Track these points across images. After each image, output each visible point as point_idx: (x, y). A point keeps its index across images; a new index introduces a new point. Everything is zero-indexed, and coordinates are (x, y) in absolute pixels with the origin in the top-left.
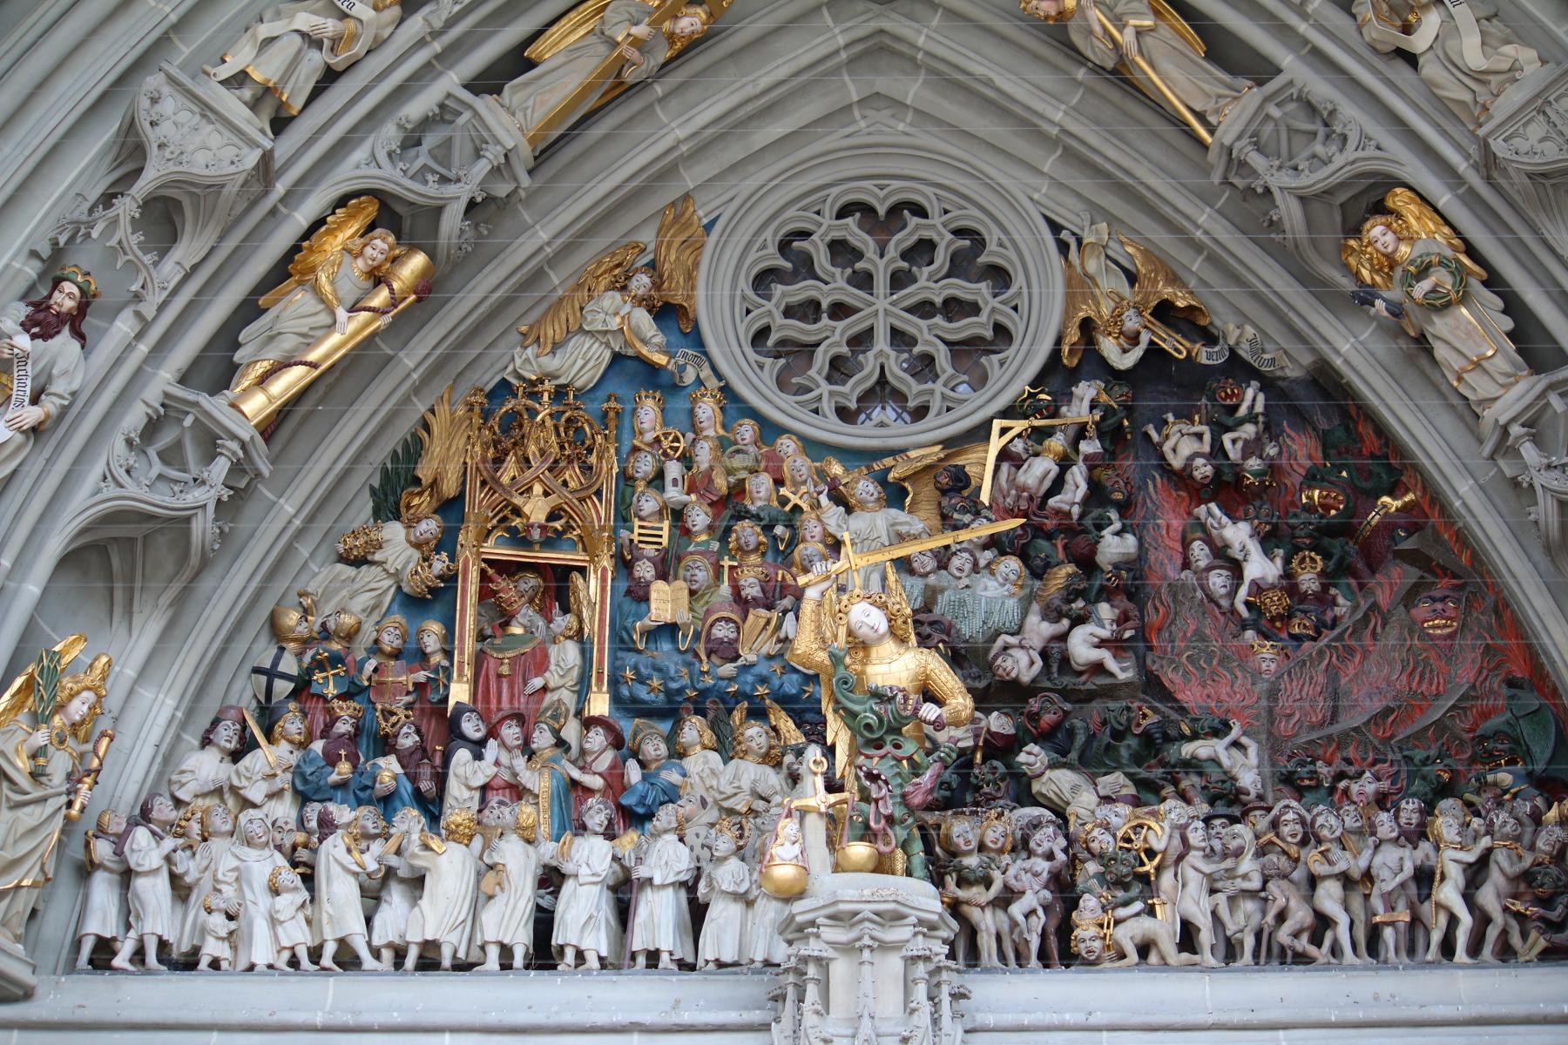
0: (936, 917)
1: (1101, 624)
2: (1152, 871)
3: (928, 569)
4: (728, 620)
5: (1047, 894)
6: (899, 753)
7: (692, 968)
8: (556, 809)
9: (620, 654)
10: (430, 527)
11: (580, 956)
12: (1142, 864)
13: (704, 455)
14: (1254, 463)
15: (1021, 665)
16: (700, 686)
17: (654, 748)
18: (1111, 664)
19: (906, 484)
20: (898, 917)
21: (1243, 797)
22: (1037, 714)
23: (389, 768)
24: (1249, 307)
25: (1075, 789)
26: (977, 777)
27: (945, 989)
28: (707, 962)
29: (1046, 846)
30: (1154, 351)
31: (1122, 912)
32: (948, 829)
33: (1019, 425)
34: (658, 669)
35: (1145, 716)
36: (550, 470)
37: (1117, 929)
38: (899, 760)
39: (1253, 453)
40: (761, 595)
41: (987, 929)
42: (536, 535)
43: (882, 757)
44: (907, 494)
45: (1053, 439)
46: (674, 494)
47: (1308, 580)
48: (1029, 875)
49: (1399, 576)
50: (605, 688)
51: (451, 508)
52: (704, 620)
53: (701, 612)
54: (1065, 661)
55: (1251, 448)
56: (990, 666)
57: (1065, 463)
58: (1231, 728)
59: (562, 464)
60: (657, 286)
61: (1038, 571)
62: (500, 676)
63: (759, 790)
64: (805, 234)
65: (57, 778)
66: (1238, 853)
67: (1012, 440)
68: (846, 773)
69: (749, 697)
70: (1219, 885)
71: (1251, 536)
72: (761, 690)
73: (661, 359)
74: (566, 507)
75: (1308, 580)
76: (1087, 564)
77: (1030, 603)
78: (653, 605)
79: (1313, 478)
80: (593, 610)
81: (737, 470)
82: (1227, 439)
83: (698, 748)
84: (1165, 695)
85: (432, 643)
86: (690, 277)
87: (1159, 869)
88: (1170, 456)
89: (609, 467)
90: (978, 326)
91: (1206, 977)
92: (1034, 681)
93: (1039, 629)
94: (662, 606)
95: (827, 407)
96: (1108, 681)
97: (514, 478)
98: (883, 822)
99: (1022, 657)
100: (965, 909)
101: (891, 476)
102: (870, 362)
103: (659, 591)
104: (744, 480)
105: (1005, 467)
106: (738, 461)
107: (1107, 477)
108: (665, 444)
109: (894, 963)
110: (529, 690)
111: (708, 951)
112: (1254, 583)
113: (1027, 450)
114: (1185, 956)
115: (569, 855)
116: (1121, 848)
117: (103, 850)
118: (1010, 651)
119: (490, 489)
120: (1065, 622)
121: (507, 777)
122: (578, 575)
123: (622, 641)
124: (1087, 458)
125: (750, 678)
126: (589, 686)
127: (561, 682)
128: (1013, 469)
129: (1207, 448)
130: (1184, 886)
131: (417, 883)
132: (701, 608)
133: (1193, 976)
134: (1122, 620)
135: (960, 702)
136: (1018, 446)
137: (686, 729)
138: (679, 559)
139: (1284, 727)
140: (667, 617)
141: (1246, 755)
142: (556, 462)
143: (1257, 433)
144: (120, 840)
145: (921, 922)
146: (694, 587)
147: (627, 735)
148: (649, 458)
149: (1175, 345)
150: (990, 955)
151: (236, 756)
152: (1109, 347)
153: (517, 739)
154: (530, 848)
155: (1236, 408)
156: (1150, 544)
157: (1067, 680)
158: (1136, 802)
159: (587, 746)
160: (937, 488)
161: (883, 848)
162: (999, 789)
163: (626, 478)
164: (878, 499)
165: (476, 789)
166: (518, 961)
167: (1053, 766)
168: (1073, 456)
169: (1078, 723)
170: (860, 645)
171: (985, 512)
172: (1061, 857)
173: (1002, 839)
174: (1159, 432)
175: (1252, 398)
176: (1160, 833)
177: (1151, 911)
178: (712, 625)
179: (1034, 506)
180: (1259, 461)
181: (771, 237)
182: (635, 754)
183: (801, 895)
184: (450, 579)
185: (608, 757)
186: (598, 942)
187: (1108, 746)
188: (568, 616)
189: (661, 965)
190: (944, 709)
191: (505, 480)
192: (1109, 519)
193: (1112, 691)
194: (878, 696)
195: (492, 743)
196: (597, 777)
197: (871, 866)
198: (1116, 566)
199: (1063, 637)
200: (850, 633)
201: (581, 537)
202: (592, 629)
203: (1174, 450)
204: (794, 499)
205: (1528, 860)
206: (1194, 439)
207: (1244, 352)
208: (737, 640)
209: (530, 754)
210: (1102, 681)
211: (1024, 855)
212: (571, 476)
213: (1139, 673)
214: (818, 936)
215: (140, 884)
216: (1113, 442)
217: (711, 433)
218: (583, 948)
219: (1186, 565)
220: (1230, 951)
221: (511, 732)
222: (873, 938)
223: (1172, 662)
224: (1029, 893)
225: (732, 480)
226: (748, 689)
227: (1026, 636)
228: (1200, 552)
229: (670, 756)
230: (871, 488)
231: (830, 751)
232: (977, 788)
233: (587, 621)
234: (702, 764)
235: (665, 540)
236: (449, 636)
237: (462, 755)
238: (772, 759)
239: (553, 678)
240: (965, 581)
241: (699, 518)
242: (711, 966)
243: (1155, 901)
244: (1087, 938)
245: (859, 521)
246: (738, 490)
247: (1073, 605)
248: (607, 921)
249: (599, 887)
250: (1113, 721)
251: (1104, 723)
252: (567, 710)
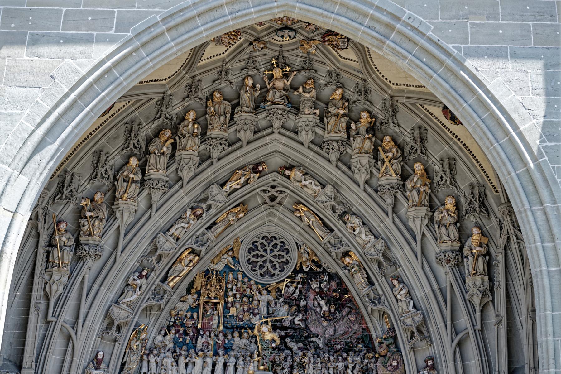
10: (196, 296)
13: (239, 285)
14: (325, 289)
15: (287, 324)
17: (229, 337)
18: (301, 324)
23: (188, 338)
24: (326, 261)
25: (294, 346)
30: (311, 269)
33: (289, 280)
46: (234, 292)
47: (332, 310)
49: (346, 310)
51: (199, 293)
54: (294, 322)
60: (233, 254)
61: (290, 306)
64: (257, 242)
65: (140, 348)
73: (233, 267)
75: (332, 310)
76: (298, 306)
79: (335, 291)
84: (309, 329)
85: (195, 316)
86: (238, 252)
89: (224, 285)
90: (284, 260)
93: (290, 318)
95: (259, 274)
102: (266, 266)
103: (232, 309)
106: (245, 286)
117: (145, 357)
131: (194, 363)
132: (238, 311)
134: (303, 316)
136: (289, 284)
139: (327, 335)
144: (148, 355)
149: (314, 268)
151: (164, 336)
152: (304, 267)
155: (322, 280)
172: (291, 363)
175: (326, 277)
177: (304, 371)
181: (251, 242)
184: (198, 305)
193: (300, 329)
198: (303, 307)
199: (294, 319)
205: (362, 366)
207: (325, 268)
210: (299, 327)
215: (151, 364)
219: (314, 305)
228: (316, 303)
234: (237, 339)
236: (198, 315)
237: (200, 337)
239: (214, 322)
241: (238, 296)
245: (263, 297)
246: (244, 291)
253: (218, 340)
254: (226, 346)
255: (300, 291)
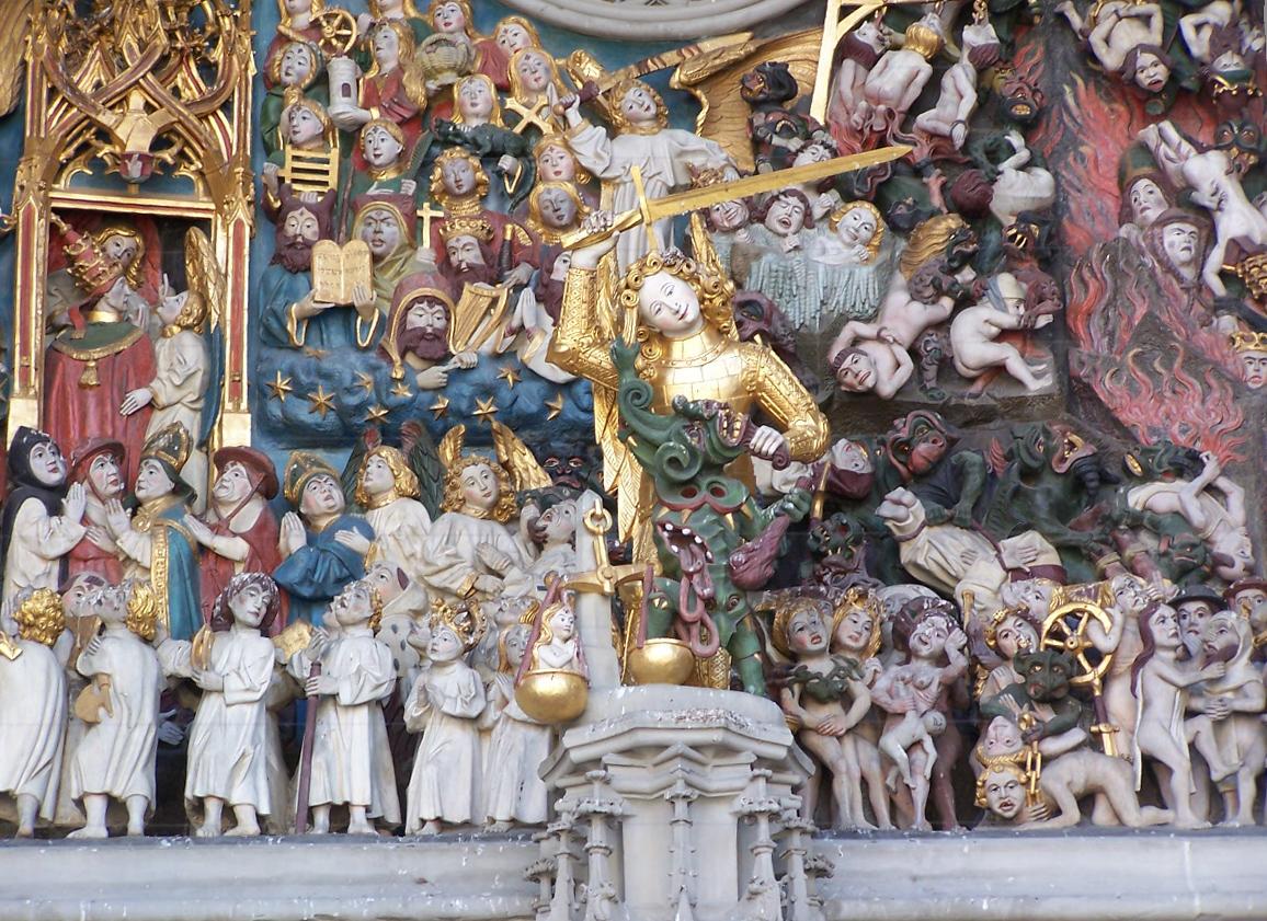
0: (782, 753)
1: (1000, 304)
2: (1097, 682)
3: (736, 222)
4: (432, 301)
5: (937, 719)
6: (721, 502)
7: (399, 831)
8: (176, 590)
9: (266, 353)
11: (228, 812)
12: (1083, 672)
13: (389, 49)
14: (1229, 62)
16: (392, 401)
17: (323, 497)
18: (1016, 366)
19: (698, 92)
20: (725, 750)
21: (1224, 570)
22: (907, 443)
25: (968, 557)
26: (817, 539)
27: (797, 866)
28: (423, 822)
29: (936, 644)
31: (1052, 745)
32: (787, 617)
34: (327, 376)
35: (1072, 445)
36: (154, 70)
37: (1048, 771)
38: (723, 513)
39: (1226, 47)
40: (481, 262)
41: (848, 771)
42: (135, 170)
43: (695, 509)
44: (700, 107)
45: (923, 22)
46: (344, 107)
48: (911, 688)
50: (244, 405)
52: (395, 301)
53: (390, 288)
54: (946, 364)
55: (1226, 38)
56: (833, 371)
57: (940, 61)
58: (1203, 465)
59: (173, 61)
61: (900, 225)
62: (83, 387)
63: (487, 560)
66: (1228, 654)
67: (858, 25)
68: (635, 533)
69: (466, 417)
70: (1197, 704)
71: (1228, 173)
72: (485, 407)
74: (179, 128)
76: (977, 213)
77: (892, 273)
78: (318, 279)
80: (224, 287)
81: (439, 71)
82: (1187, 23)
83: (391, 495)
87: (1105, 679)
88: (1100, 50)
91: (1186, 844)
92: (899, 391)
93: (906, 314)
94: (331, 279)
96: (1014, 393)
97: (98, 85)
98: (700, 605)
99: (881, 355)
100: (814, 740)
101: (676, 79)
103: (326, 256)
104: (451, 86)
105: (849, 64)
106: (441, 56)
107: (1003, 83)
108: (328, 30)
109: (722, 819)
110: (127, 409)
111: (423, 804)
112: (1233, 242)
113: (881, 40)
114: (1151, 813)
115: (208, 659)
116: (1047, 646)
118: (863, 347)
119: (64, 100)
120: (947, 303)
121: (101, 542)
122: (200, 233)
123: (268, 331)
124: (975, 54)
125: (467, 390)
126: (219, 402)
127: (177, 395)
128: (862, 70)
129: (1155, 38)
130: (1146, 705)
132: (389, 281)
133: (1165, 841)
134: (1032, 300)
135: (807, 423)
136: (868, 35)
137: (373, 468)
138: (354, 208)
140: (342, 298)
141: (1226, 506)
142: (165, 59)
143: (1233, 16)
145: (761, 761)
146: (378, 250)
147: (283, 475)
148: (306, 53)
150: (852, 809)
153: (115, 483)
154: (147, 650)
156: (1068, 182)
157: (949, 392)
158: (1061, 576)
159: (222, 493)
160: (746, 99)
161: (700, 649)
162: (851, 556)
163: (269, 84)
164: (657, 117)
165: (54, 559)
166: (136, 823)
167: (929, 523)
168: (952, 49)
169: (972, 457)
170: (656, 335)
171: (818, 135)
173: (865, 633)
174: (1082, 15)
176: (1107, 624)
177: (1095, 743)
178: (408, 308)
179: (895, 125)
180: (1236, 59)
182: (293, 505)
183: (574, 721)
185: (252, 514)
186: (253, 794)
187: (1017, 493)
188: (184, 294)
189: (351, 829)
190: (787, 436)
191: (86, 86)
192: (1010, 145)
193: (1018, 407)
194: (691, 415)
195: (77, 490)
196: (239, 539)
197: (682, 676)
198: (1023, 218)
199: (943, 325)
200: (642, 320)
201: (200, 173)
202: (222, 315)
203: (1107, 40)
204: (529, 116)
206: (1136, 24)
208: (446, 330)
209: (135, 506)
210: (1005, 392)
211: (898, 656)
212: (184, 80)
213: (1060, 381)
214: (606, 781)
216: (1012, 29)
217: (396, 13)
218: (233, 801)
219: (1126, 214)
220: (1217, 798)
221: (104, 473)
222: (689, 784)
223: (1109, 362)
224: (911, 715)
225: (432, 85)
226: (464, 405)
227: (886, 323)
228: (1147, 195)
229: (345, 511)
230: (648, 102)
231: (610, 504)
232: (819, 556)
233: (215, 302)
235: (332, 179)
237: (31, 510)
238: (502, 512)
239: (163, 389)
240: (792, 241)
241: (384, 143)
242: (430, 829)
243: (1102, 727)
244: (1002, 784)
246: (443, 97)
247: (958, 277)
248: (267, 764)
249: (256, 706)
250: (1024, 454)
251: (1010, 456)
252: (190, 439)
253: (219, 528)
254: (293, 576)
255: (985, 95)
